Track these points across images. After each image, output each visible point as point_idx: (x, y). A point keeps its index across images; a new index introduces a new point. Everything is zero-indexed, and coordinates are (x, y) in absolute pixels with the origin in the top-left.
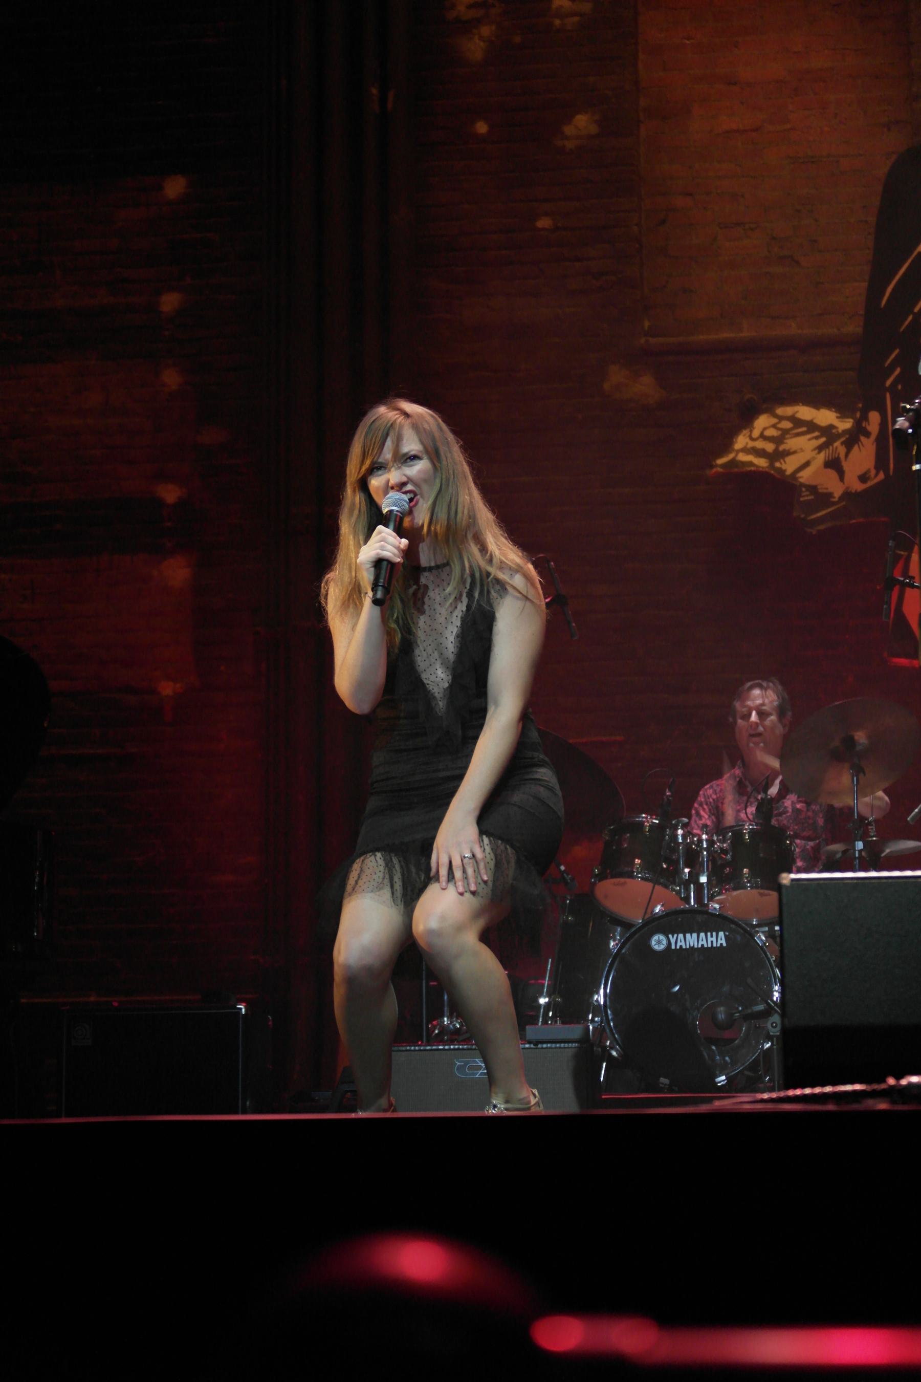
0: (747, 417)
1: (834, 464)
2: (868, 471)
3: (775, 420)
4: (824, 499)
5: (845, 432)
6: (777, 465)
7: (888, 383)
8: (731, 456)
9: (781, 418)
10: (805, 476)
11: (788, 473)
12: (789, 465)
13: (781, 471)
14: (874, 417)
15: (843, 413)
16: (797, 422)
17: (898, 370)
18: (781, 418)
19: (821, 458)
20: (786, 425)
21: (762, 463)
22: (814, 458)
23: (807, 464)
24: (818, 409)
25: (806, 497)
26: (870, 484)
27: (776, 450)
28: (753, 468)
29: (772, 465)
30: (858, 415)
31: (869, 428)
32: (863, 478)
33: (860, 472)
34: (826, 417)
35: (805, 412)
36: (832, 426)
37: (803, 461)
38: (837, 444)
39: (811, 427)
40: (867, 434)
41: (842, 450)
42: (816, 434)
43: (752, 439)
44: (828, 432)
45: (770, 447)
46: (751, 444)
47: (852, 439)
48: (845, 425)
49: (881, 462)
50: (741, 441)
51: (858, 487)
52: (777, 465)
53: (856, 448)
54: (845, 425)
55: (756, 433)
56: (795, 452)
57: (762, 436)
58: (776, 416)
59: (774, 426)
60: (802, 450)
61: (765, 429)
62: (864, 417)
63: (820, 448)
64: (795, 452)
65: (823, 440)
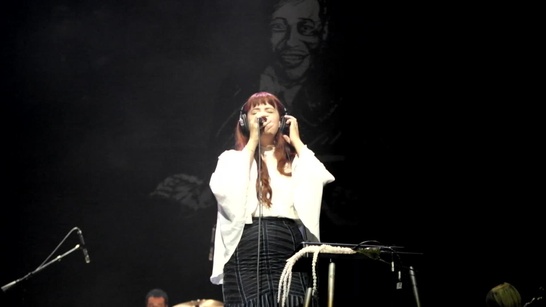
12: (178, 197)
20: (177, 181)
21: (167, 195)
23: (184, 197)
35: (185, 177)
36: (195, 183)
39: (187, 183)
45: (170, 189)
50: (160, 187)
63: (190, 191)
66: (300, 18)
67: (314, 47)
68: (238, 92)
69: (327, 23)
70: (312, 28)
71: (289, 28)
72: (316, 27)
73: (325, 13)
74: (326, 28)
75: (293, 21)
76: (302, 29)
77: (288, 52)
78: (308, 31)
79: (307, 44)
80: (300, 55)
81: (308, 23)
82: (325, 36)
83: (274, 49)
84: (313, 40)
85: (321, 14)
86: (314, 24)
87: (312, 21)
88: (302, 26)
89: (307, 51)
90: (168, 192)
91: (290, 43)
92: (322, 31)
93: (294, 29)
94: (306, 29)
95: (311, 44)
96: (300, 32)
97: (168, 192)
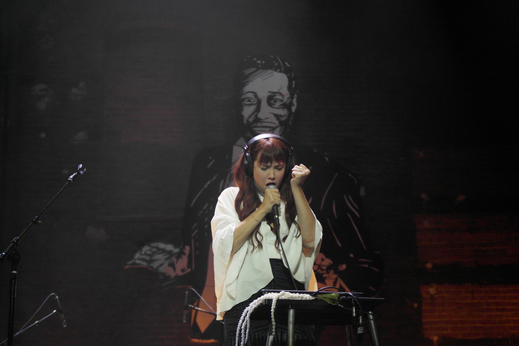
0: (141, 245)
1: (172, 265)
3: (149, 248)
4: (167, 278)
6: (151, 265)
7: (193, 235)
9: (153, 247)
10: (161, 269)
12: (155, 265)
13: (152, 267)
14: (187, 248)
15: (176, 246)
16: (158, 249)
17: (196, 231)
18: (153, 247)
19: (167, 263)
20: (154, 250)
21: (145, 264)
23: (161, 265)
26: (184, 273)
28: (140, 266)
30: (181, 247)
32: (183, 270)
34: (169, 247)
35: (162, 245)
39: (164, 251)
40: (184, 254)
42: (165, 254)
44: (170, 253)
45: (148, 258)
46: (141, 257)
48: (176, 250)
49: (189, 264)
50: (137, 256)
51: (180, 273)
52: (151, 265)
53: (180, 260)
54: (176, 250)
55: (143, 253)
57: (145, 254)
59: (150, 250)
61: (146, 251)
62: (184, 248)
63: (167, 259)
65: (167, 256)
66: (269, 92)
67: (283, 119)
68: (211, 163)
69: (296, 96)
70: (281, 101)
71: (259, 102)
72: (285, 100)
73: (293, 86)
74: (295, 101)
75: (263, 95)
76: (272, 102)
77: (259, 124)
78: (278, 104)
79: (277, 116)
80: (270, 127)
81: (278, 97)
82: (294, 109)
83: (245, 122)
84: (283, 112)
85: (290, 88)
86: (283, 97)
87: (281, 94)
88: (271, 99)
89: (277, 123)
90: (144, 260)
91: (260, 115)
92: (291, 104)
93: (264, 103)
94: (275, 102)
95: (282, 116)
96: (270, 105)
97: (144, 260)
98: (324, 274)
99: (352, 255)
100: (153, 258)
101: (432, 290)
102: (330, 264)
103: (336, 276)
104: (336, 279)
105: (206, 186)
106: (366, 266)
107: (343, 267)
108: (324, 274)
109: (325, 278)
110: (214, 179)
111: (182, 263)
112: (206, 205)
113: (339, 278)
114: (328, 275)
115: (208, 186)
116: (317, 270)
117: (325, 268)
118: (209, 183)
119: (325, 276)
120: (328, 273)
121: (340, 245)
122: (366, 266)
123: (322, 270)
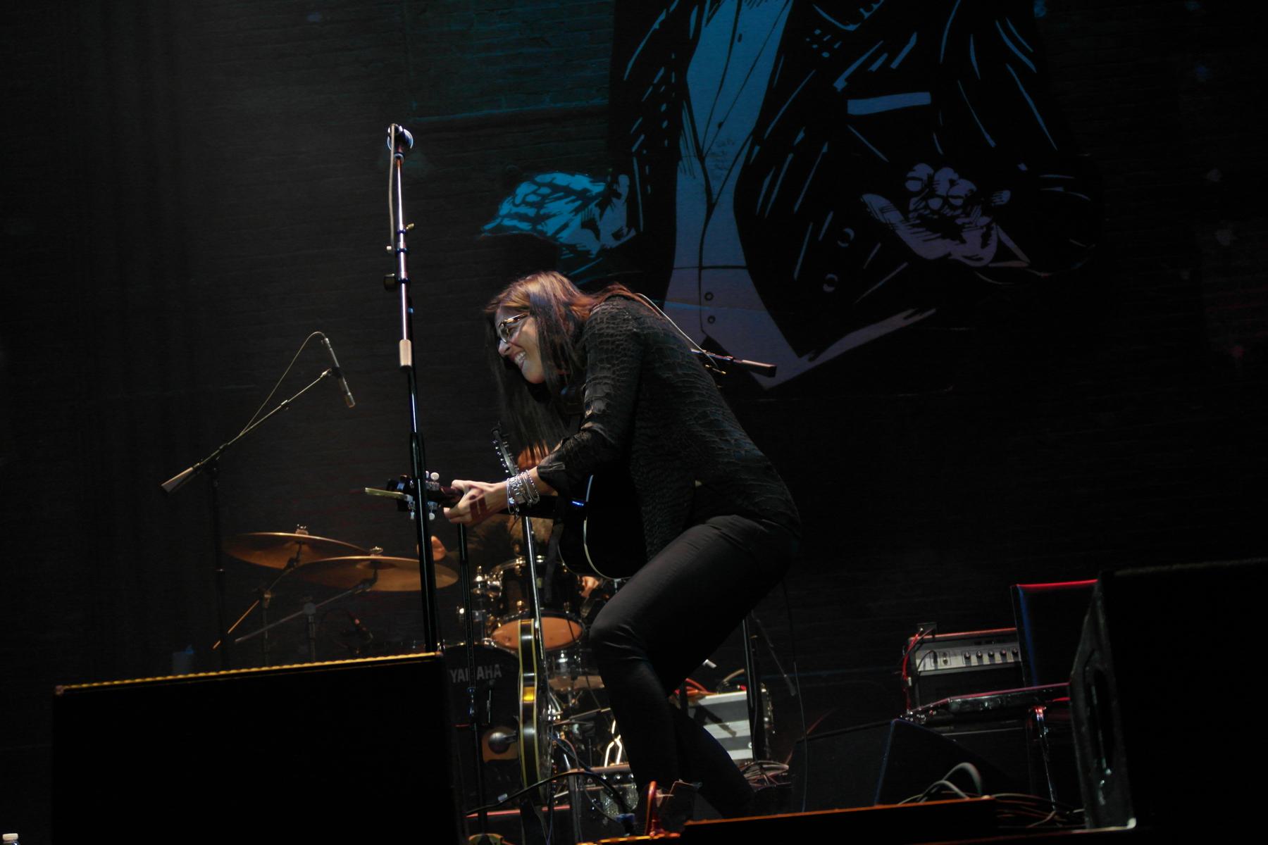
1: (590, 224)
2: (621, 230)
3: (535, 187)
5: (599, 195)
6: (539, 227)
7: (634, 149)
8: (498, 221)
9: (540, 185)
10: (564, 236)
11: (550, 233)
12: (550, 227)
13: (542, 233)
14: (624, 180)
15: (595, 178)
16: (555, 188)
17: (642, 137)
18: (540, 185)
19: (578, 220)
20: (545, 191)
21: (525, 226)
22: (571, 220)
24: (573, 174)
25: (567, 255)
26: (624, 239)
27: (537, 215)
29: (534, 229)
30: (609, 179)
31: (620, 190)
32: (617, 236)
33: (615, 229)
34: (580, 182)
35: (561, 179)
36: (585, 191)
37: (562, 223)
38: (592, 206)
39: (568, 191)
40: (618, 196)
41: (596, 211)
42: (573, 197)
43: (517, 206)
44: (583, 195)
45: (531, 212)
46: (515, 210)
47: (605, 201)
48: (598, 188)
49: (632, 220)
50: (506, 208)
51: (613, 243)
52: (539, 227)
54: (598, 188)
55: (518, 201)
56: (554, 215)
57: (524, 202)
58: (536, 183)
59: (534, 193)
60: (561, 214)
62: (615, 180)
63: (577, 211)
64: (554, 215)
65: (579, 203)
98: (958, 217)
99: (1023, 167)
100: (542, 212)
101: (1224, 237)
102: (971, 191)
103: (985, 220)
104: (989, 227)
105: (656, 26)
106: (1060, 189)
107: (1006, 196)
108: (958, 217)
109: (962, 227)
110: (673, 8)
111: (614, 218)
112: (662, 72)
113: (994, 225)
114: (967, 220)
115: (662, 24)
116: (942, 207)
117: (959, 202)
118: (662, 17)
119: (959, 221)
120: (968, 215)
121: (992, 143)
122: (1060, 189)
123: (954, 208)
